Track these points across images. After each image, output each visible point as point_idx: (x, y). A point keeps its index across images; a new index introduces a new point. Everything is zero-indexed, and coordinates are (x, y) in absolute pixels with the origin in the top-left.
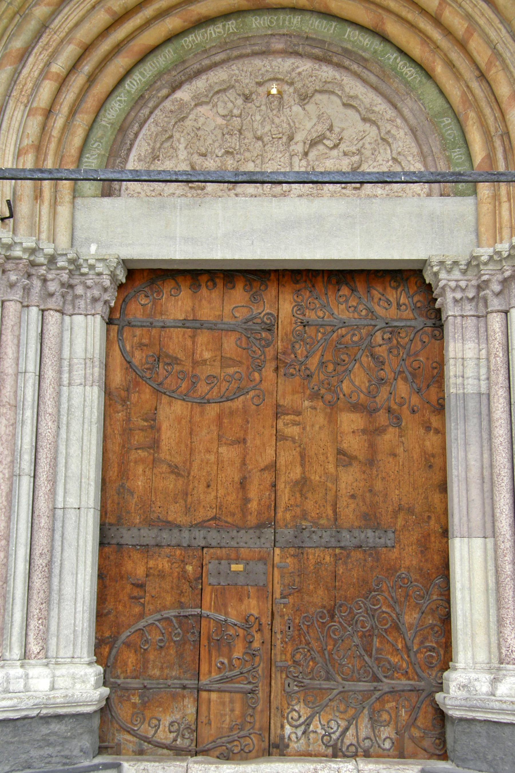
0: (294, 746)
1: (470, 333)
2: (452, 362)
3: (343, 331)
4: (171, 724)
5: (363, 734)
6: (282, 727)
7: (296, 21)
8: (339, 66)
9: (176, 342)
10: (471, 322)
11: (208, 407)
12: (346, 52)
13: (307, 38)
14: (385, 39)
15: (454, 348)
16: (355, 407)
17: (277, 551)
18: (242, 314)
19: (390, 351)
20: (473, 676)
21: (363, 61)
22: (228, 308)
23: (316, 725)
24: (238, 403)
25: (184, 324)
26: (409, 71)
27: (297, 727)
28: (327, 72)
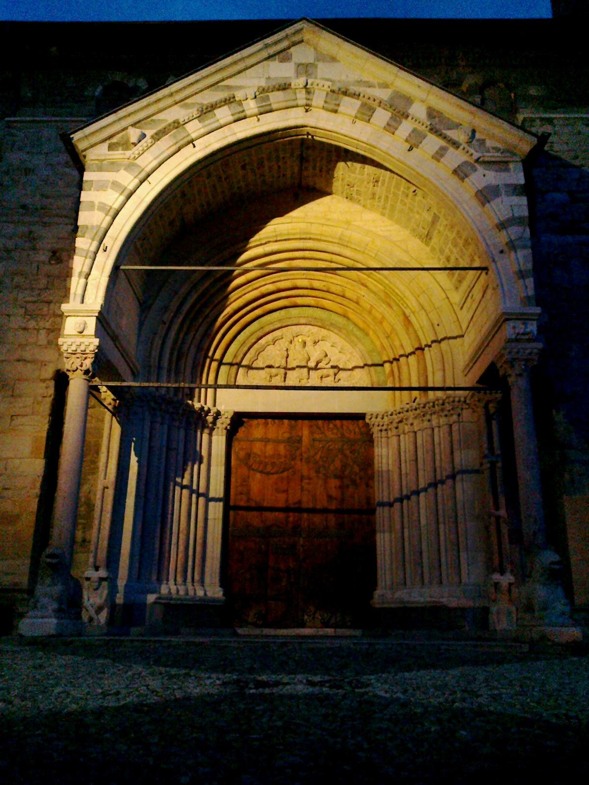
0: (308, 624)
1: (384, 445)
2: (376, 458)
3: (330, 444)
4: (255, 614)
5: (338, 619)
6: (303, 616)
7: (310, 310)
8: (328, 330)
9: (257, 448)
10: (384, 440)
11: (271, 476)
12: (332, 324)
13: (315, 318)
14: (348, 318)
15: (377, 451)
16: (336, 477)
17: (301, 539)
18: (287, 435)
19: (351, 452)
20: (385, 591)
21: (340, 329)
22: (280, 433)
23: (317, 615)
24: (285, 474)
25: (261, 440)
26: (358, 333)
27: (310, 616)
28: (324, 332)
